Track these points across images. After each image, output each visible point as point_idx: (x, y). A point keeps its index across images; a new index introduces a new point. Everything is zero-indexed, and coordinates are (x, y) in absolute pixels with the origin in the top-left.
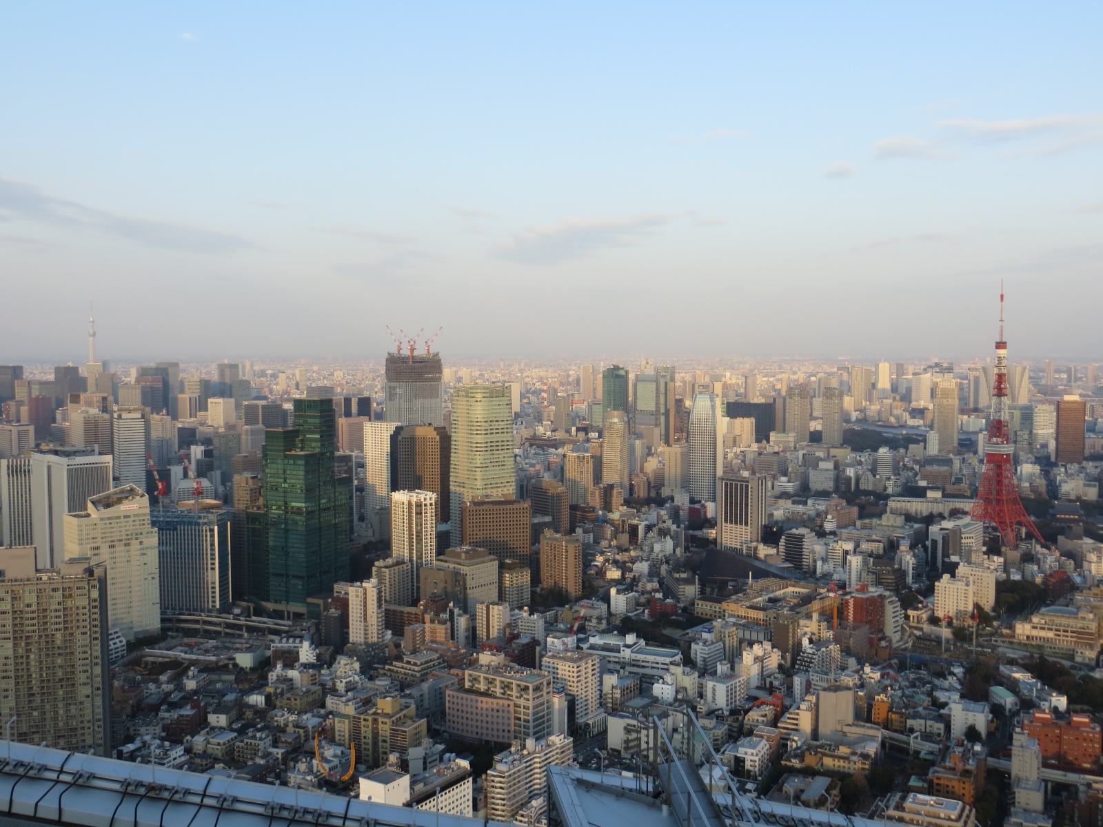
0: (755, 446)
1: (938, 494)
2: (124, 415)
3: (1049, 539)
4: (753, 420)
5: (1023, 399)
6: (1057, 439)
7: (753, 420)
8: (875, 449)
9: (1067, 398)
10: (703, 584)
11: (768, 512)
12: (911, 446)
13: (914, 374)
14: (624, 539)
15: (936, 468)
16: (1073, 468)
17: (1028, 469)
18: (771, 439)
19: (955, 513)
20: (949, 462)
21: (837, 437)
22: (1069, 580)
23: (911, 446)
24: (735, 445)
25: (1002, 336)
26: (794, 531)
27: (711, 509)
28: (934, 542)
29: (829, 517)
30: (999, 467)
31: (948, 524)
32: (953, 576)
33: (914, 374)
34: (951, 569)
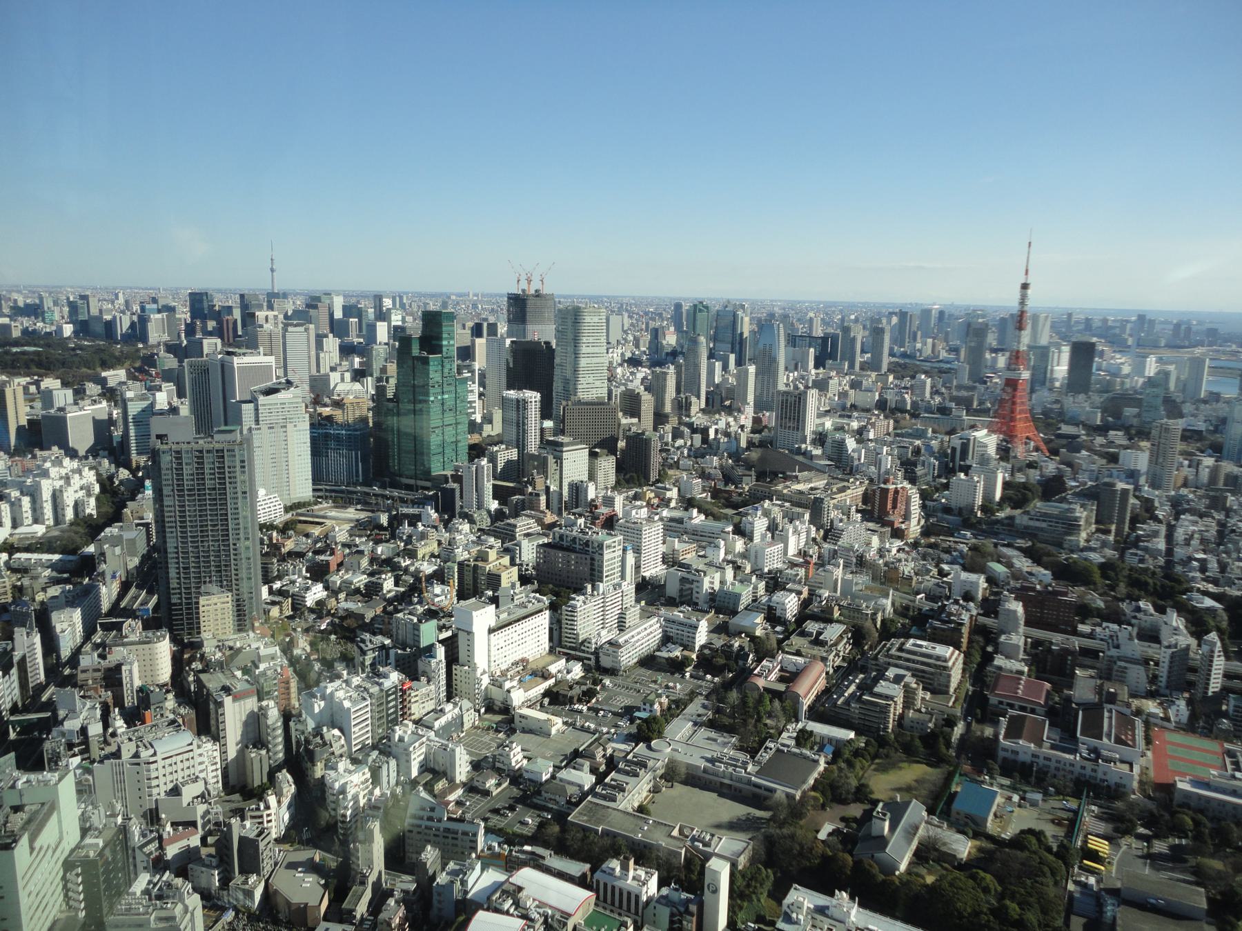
0: (813, 372)
2: (290, 329)
3: (1054, 452)
5: (1044, 341)
8: (913, 377)
10: (761, 476)
11: (818, 421)
14: (698, 438)
16: (1081, 397)
19: (973, 427)
21: (885, 367)
22: (1064, 483)
24: (796, 369)
27: (770, 418)
28: (954, 449)
30: (1015, 390)
32: (966, 475)
34: (966, 469)
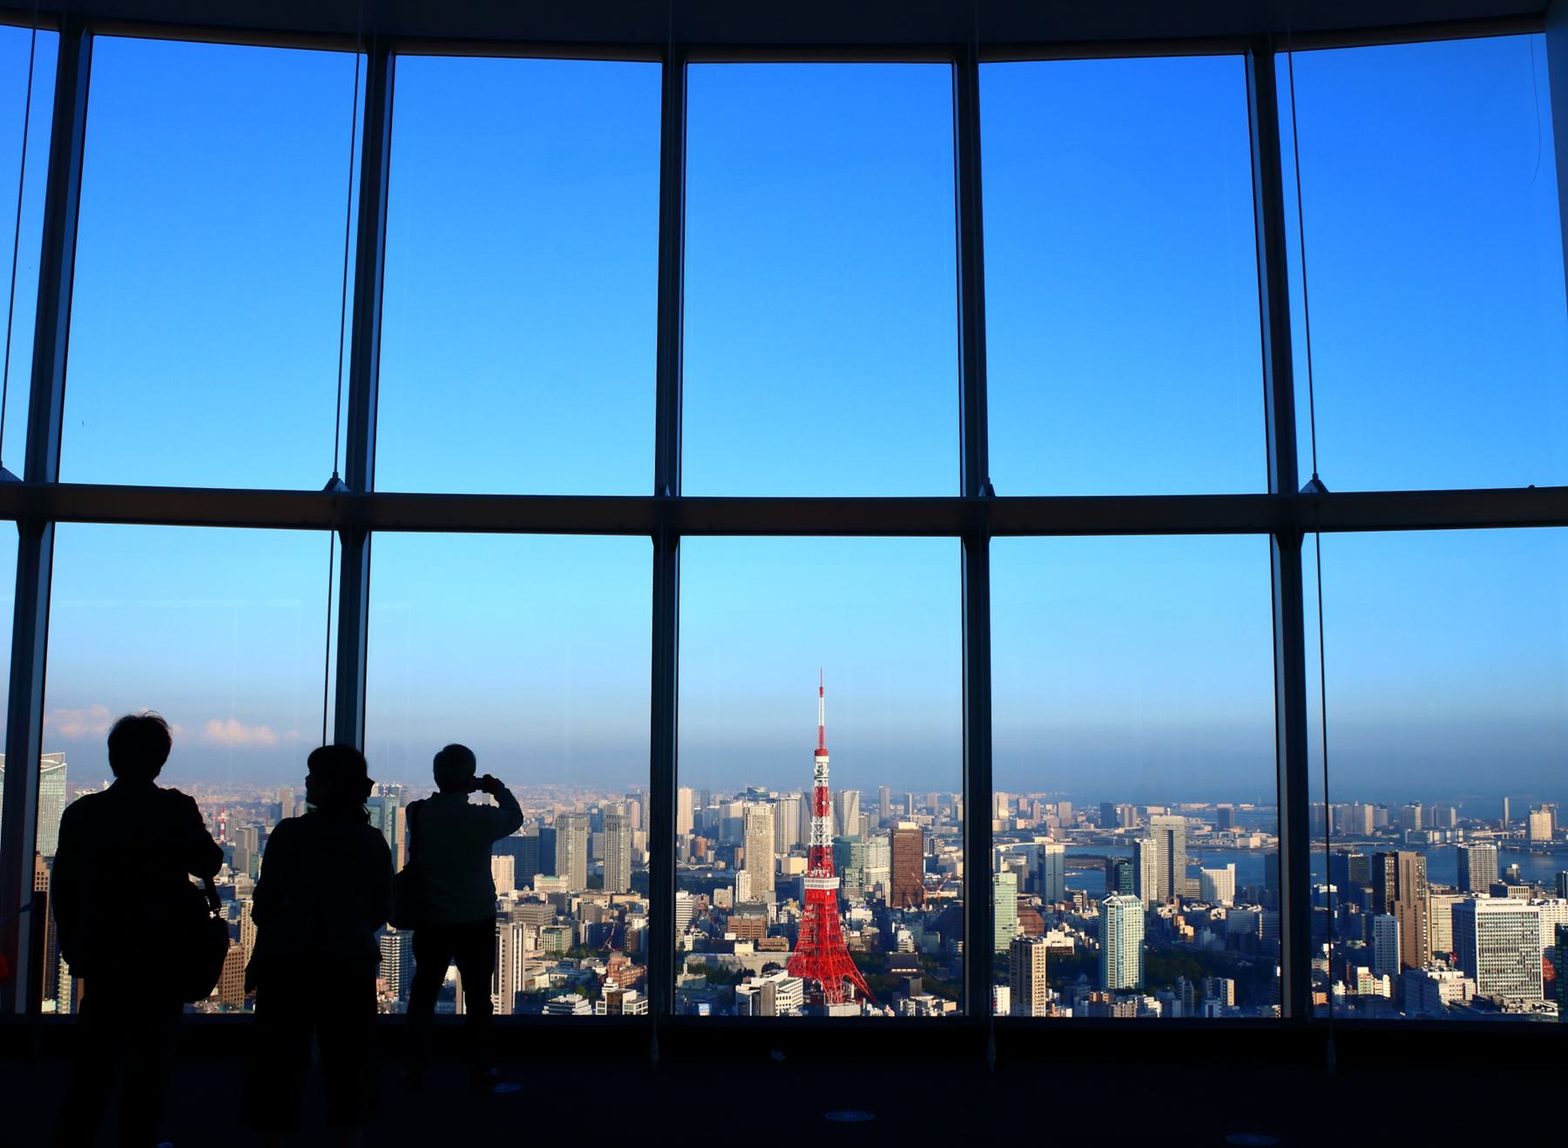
1: (749, 948)
4: (511, 858)
6: (892, 880)
7: (511, 858)
9: (903, 825)
12: (716, 891)
13: (722, 803)
15: (746, 916)
17: (860, 913)
18: (537, 884)
20: (763, 908)
23: (716, 891)
25: (821, 741)
26: (562, 999)
29: (609, 980)
31: (757, 982)
33: (722, 803)
